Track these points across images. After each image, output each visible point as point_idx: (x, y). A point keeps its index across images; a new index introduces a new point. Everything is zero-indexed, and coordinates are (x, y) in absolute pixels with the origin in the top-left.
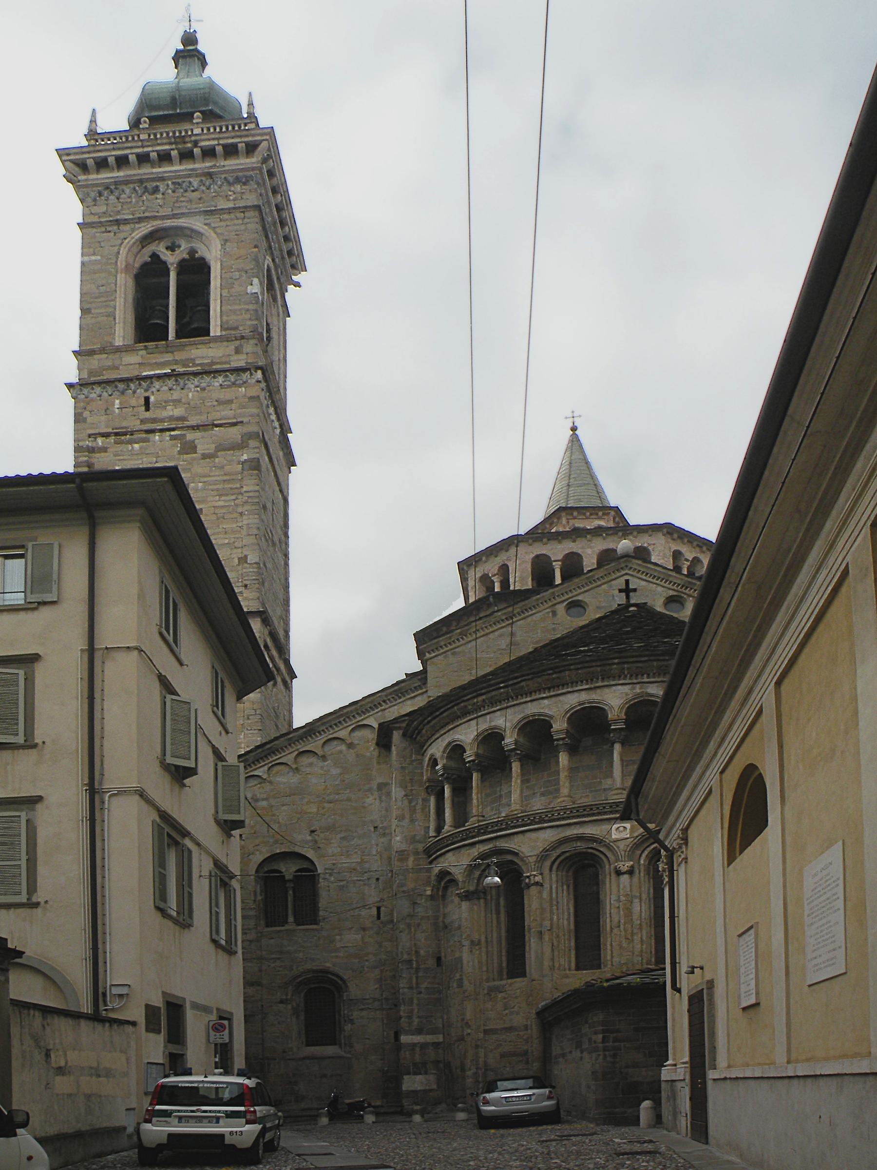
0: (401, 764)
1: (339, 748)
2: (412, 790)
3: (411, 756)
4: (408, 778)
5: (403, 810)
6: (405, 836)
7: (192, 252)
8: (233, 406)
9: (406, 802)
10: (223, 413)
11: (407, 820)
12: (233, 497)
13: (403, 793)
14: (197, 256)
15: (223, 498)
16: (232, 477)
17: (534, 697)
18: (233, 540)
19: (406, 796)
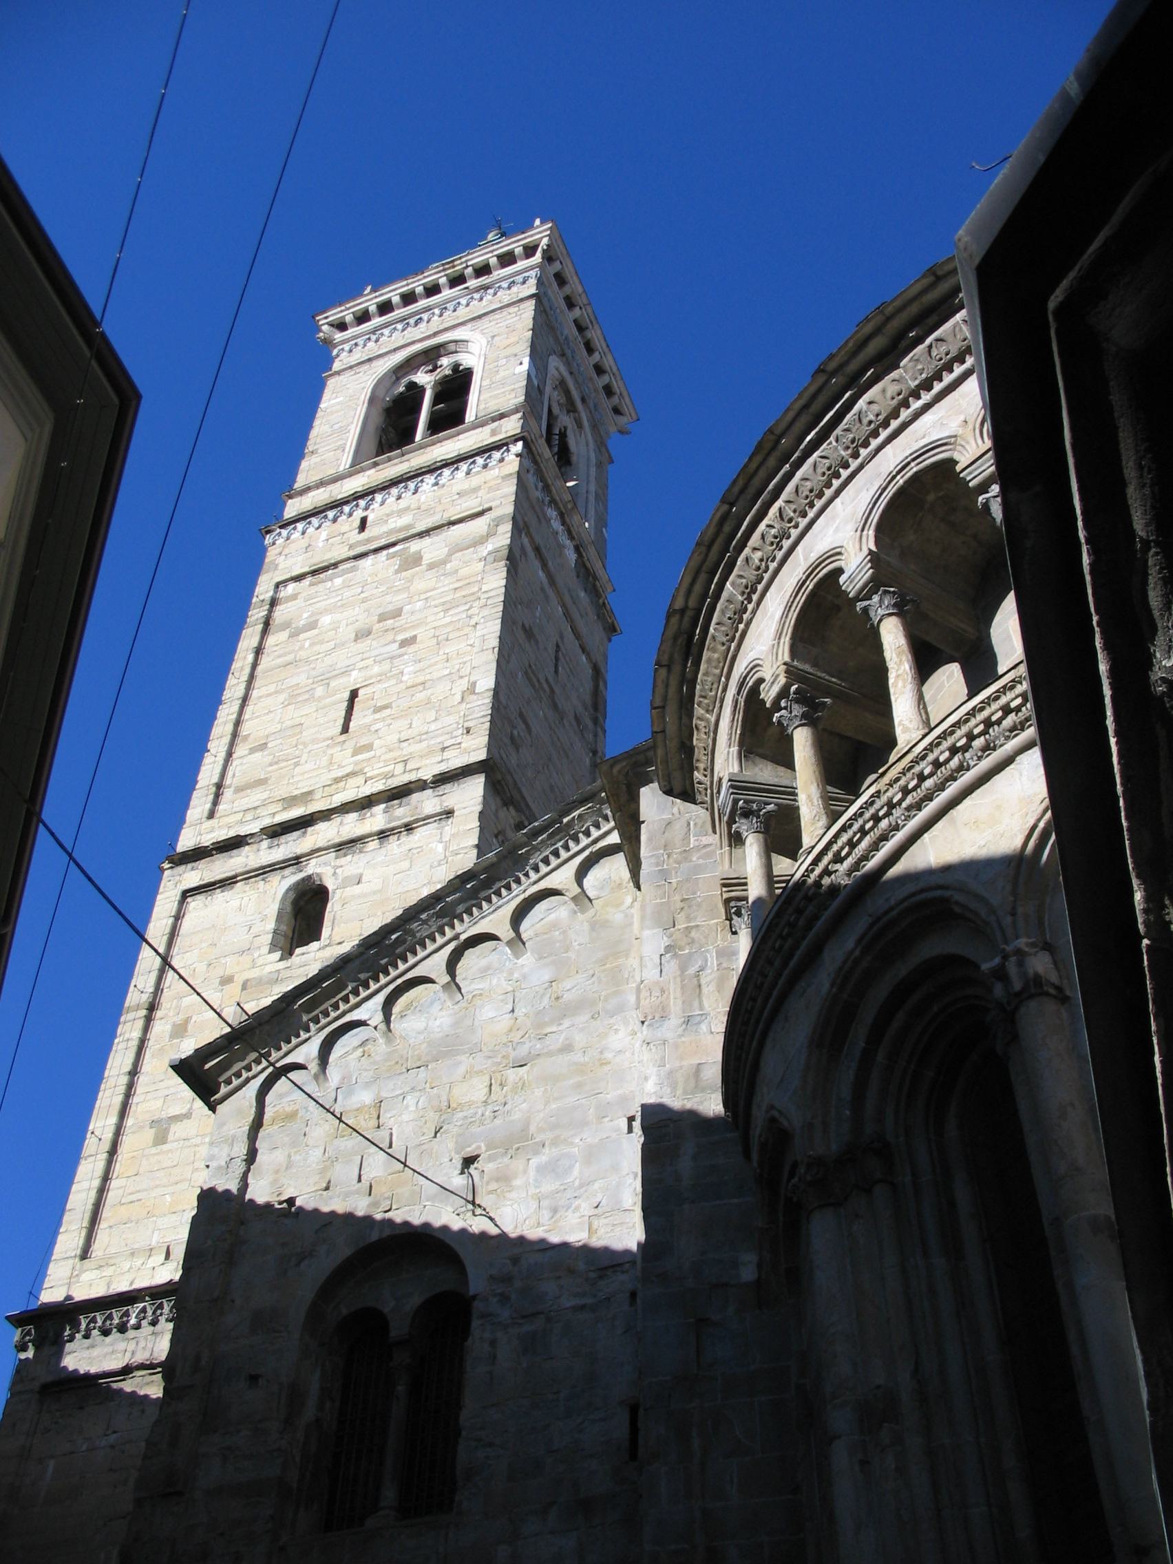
0: (657, 864)
1: (553, 916)
2: (688, 930)
3: (686, 837)
4: (677, 898)
5: (663, 991)
6: (671, 1072)
7: (456, 367)
8: (480, 493)
9: (672, 966)
10: (464, 505)
11: (674, 1021)
12: (467, 607)
13: (666, 941)
14: (461, 368)
15: (451, 612)
16: (467, 581)
17: (894, 424)
18: (457, 667)
19: (668, 949)
